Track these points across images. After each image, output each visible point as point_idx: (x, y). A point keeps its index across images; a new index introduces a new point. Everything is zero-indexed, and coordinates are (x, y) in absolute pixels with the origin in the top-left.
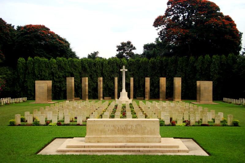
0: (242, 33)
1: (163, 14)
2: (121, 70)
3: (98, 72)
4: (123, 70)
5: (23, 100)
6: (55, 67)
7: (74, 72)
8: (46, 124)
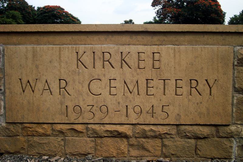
0: (226, 13)
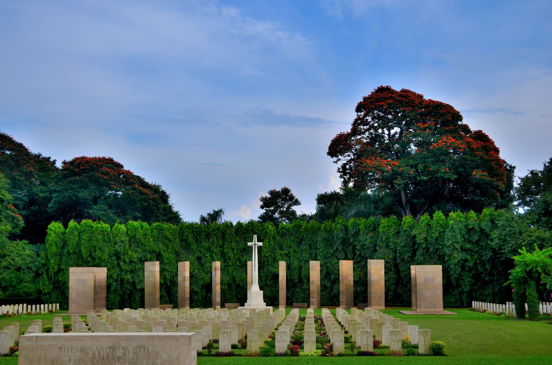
0: (514, 167)
1: (347, 129)
2: (249, 244)
3: (213, 252)
4: (253, 243)
5: (50, 308)
6: (122, 242)
7: (164, 251)
8: (10, 353)
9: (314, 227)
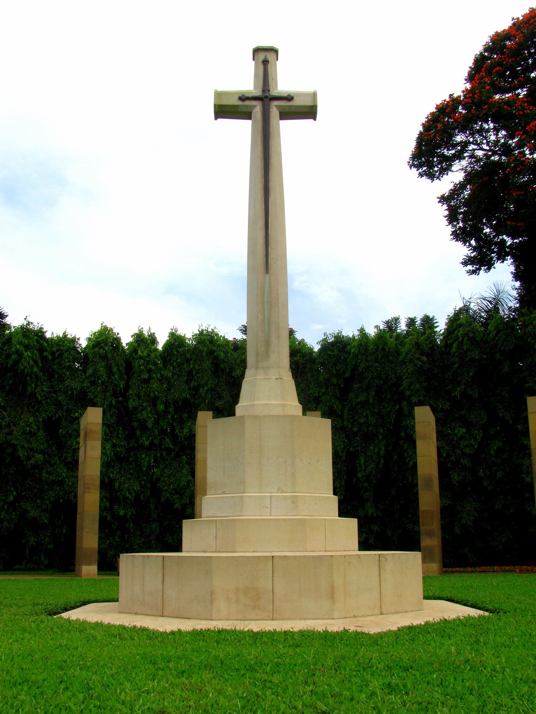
9: (385, 343)
